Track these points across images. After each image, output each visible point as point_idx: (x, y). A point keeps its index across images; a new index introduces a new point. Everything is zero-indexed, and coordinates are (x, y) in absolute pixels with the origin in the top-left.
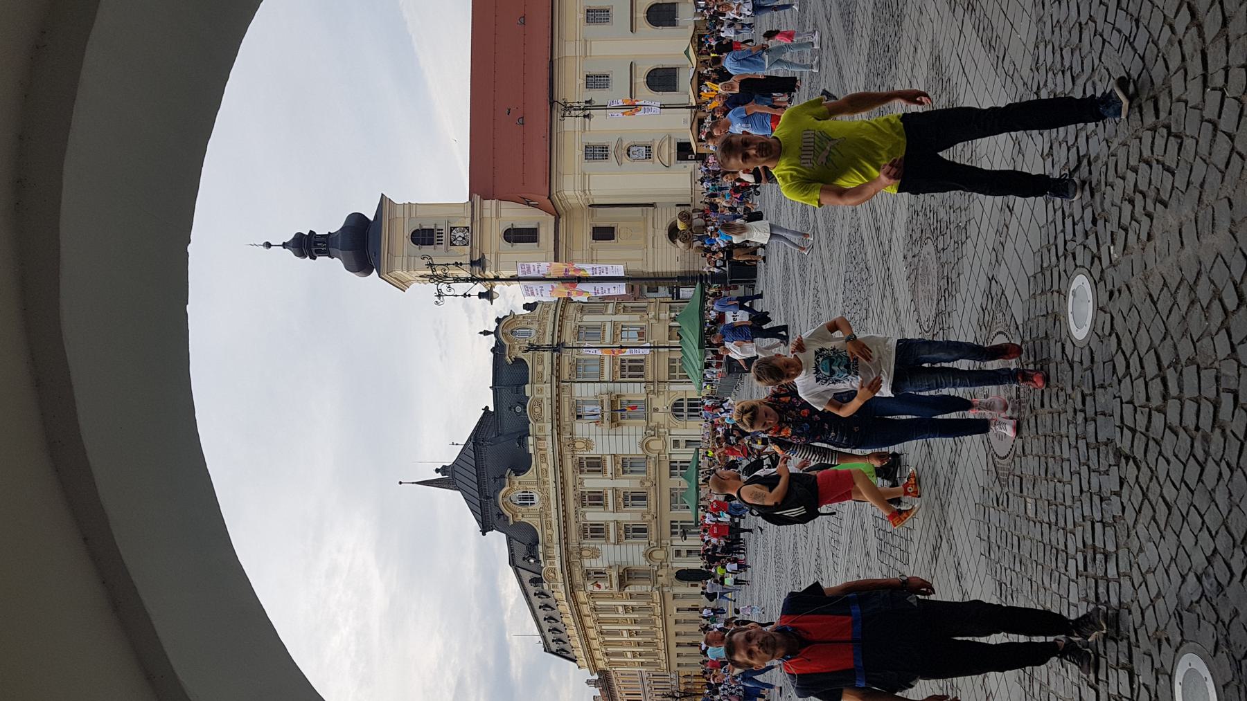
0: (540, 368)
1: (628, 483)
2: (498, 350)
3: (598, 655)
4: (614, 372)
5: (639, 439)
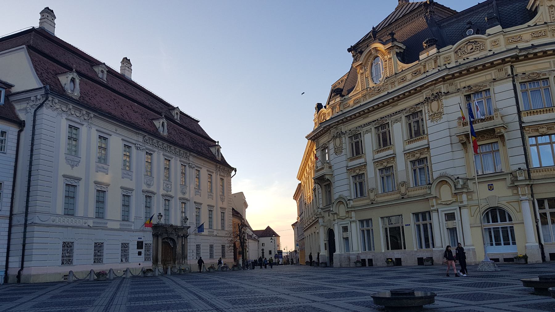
5: (450, 172)
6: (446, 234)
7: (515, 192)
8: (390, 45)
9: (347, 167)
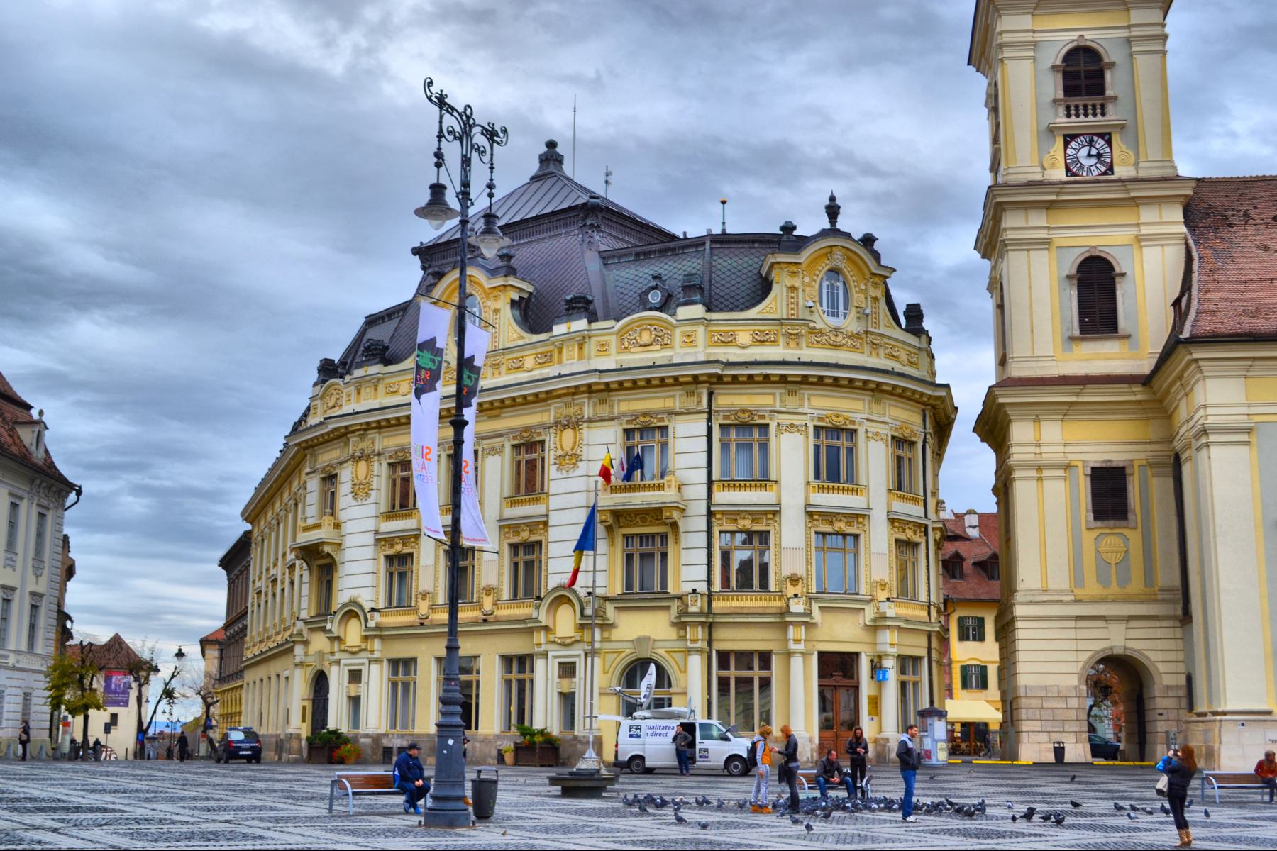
0: (744, 337)
2: (787, 240)
4: (733, 514)
6: (555, 700)
7: (682, 633)
8: (499, 281)
9: (377, 532)
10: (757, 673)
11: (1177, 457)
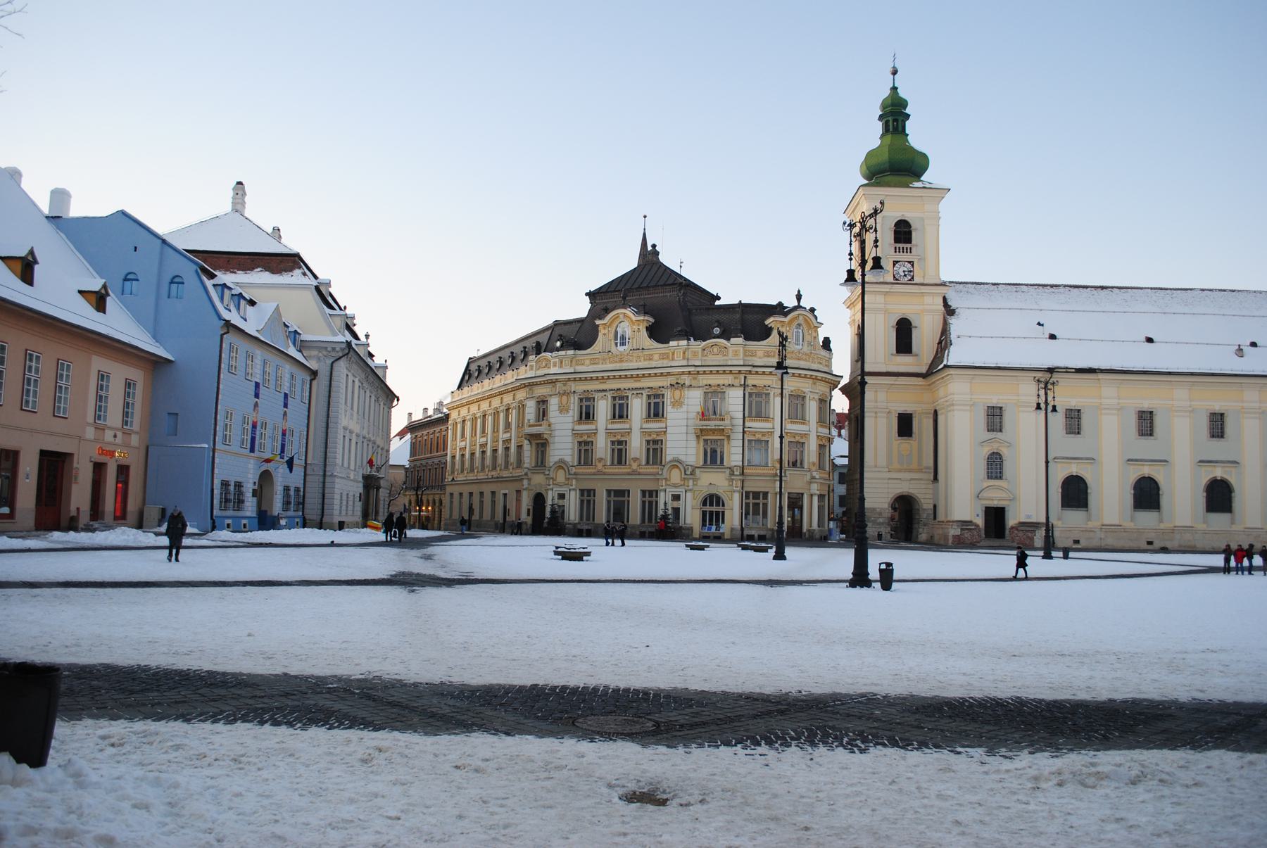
0: (760, 354)
1: (636, 446)
2: (779, 309)
3: (464, 411)
5: (682, 458)
10: (761, 501)
11: (936, 411)
